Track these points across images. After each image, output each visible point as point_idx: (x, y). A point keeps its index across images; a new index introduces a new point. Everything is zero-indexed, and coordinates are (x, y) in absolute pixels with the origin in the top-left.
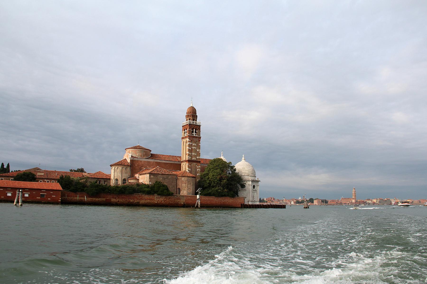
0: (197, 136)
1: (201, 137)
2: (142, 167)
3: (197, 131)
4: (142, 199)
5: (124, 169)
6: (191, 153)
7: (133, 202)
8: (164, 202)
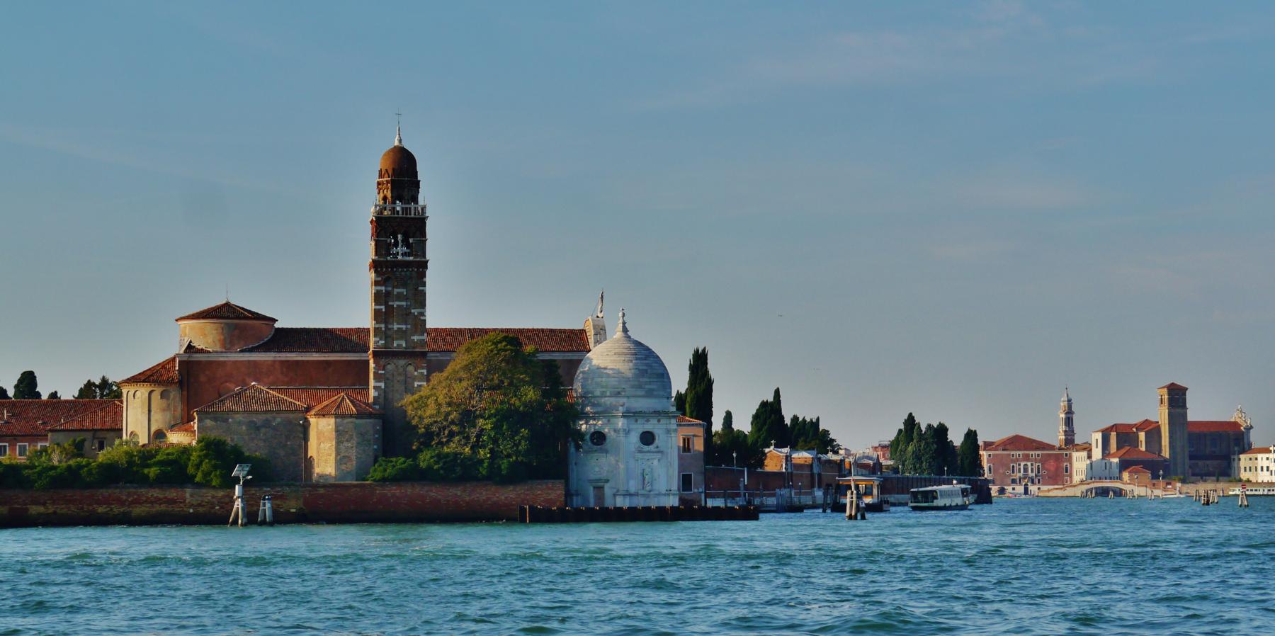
0: (411, 258)
1: (427, 261)
2: (227, 384)
3: (411, 240)
4: (140, 503)
5: (156, 396)
6: (386, 323)
7: (107, 513)
8: (222, 508)
